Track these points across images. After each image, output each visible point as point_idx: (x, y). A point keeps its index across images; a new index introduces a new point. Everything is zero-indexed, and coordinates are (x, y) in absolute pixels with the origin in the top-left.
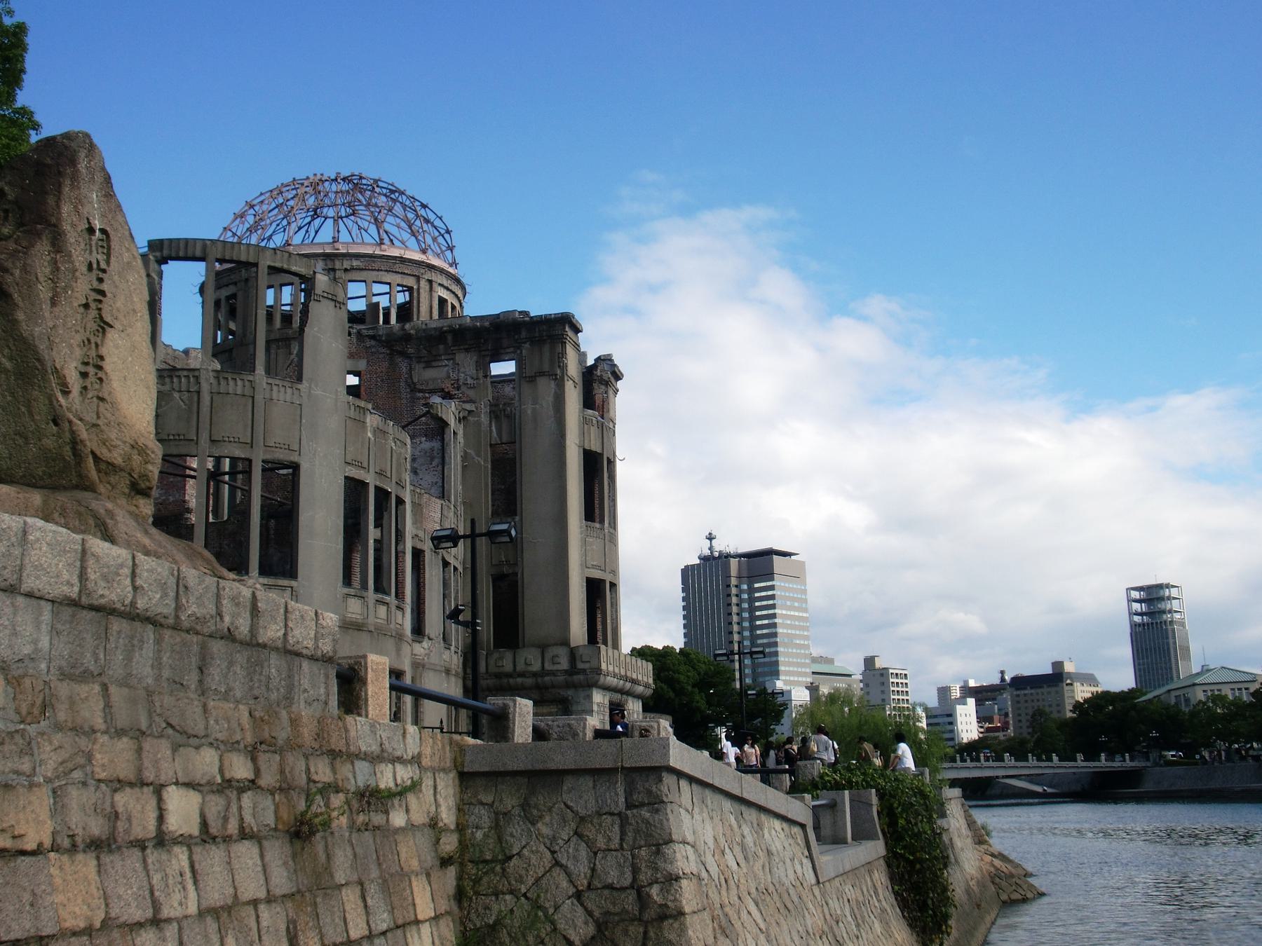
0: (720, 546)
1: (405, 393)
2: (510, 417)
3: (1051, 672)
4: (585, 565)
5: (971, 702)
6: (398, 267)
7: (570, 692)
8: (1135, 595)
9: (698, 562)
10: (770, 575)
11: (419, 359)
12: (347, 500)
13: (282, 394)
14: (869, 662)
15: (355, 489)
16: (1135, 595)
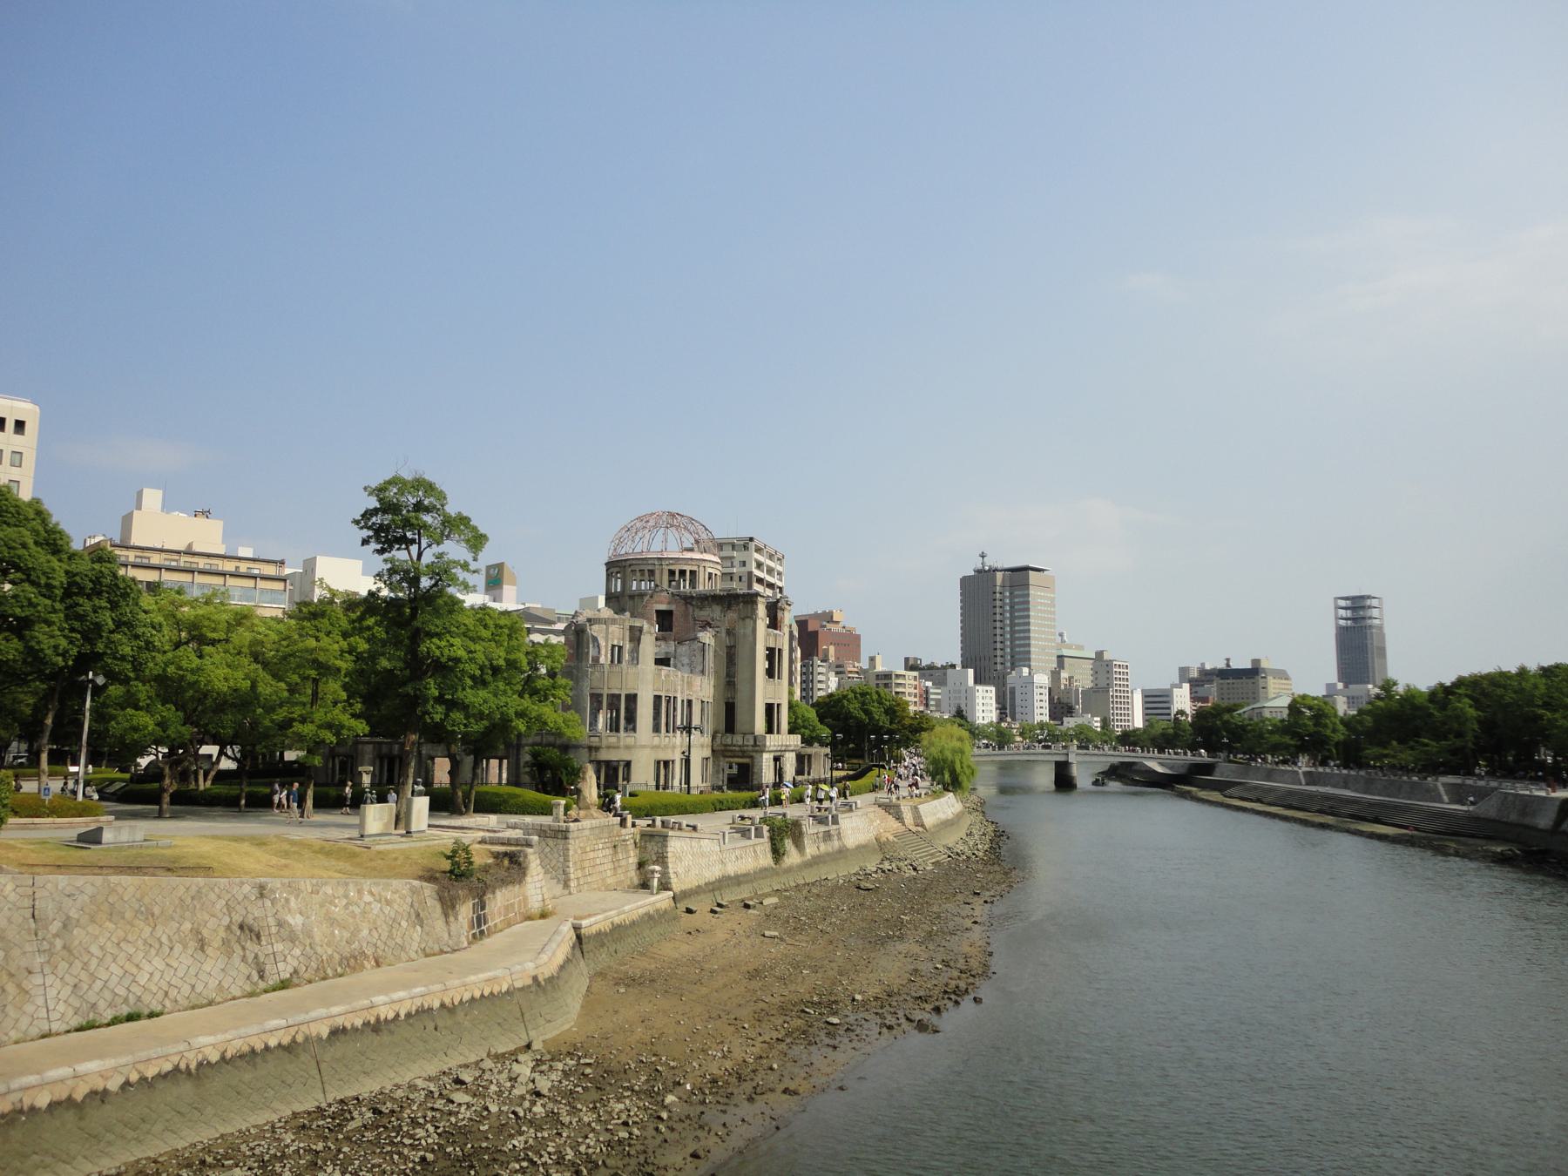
0: (991, 562)
1: (692, 622)
2: (734, 635)
3: (1250, 667)
4: (765, 698)
5: (1186, 686)
6: (690, 562)
7: (754, 754)
8: (1342, 603)
9: (973, 573)
10: (1026, 585)
11: (698, 607)
12: (655, 702)
13: (632, 670)
14: (1100, 654)
15: (657, 699)
16: (1342, 603)
